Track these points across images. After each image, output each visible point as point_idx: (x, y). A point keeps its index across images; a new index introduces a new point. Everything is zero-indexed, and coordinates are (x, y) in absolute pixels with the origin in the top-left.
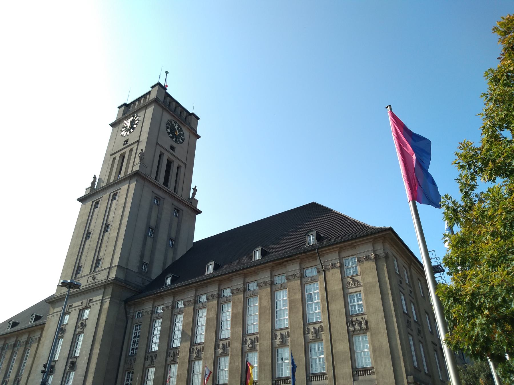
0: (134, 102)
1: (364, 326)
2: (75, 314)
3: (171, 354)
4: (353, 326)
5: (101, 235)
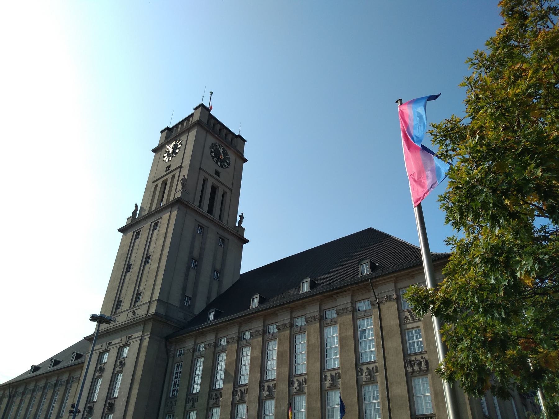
0: (176, 126)
1: (423, 366)
2: (114, 351)
3: (213, 396)
4: (412, 366)
5: (142, 267)
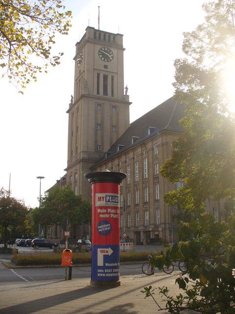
0: (81, 41)
